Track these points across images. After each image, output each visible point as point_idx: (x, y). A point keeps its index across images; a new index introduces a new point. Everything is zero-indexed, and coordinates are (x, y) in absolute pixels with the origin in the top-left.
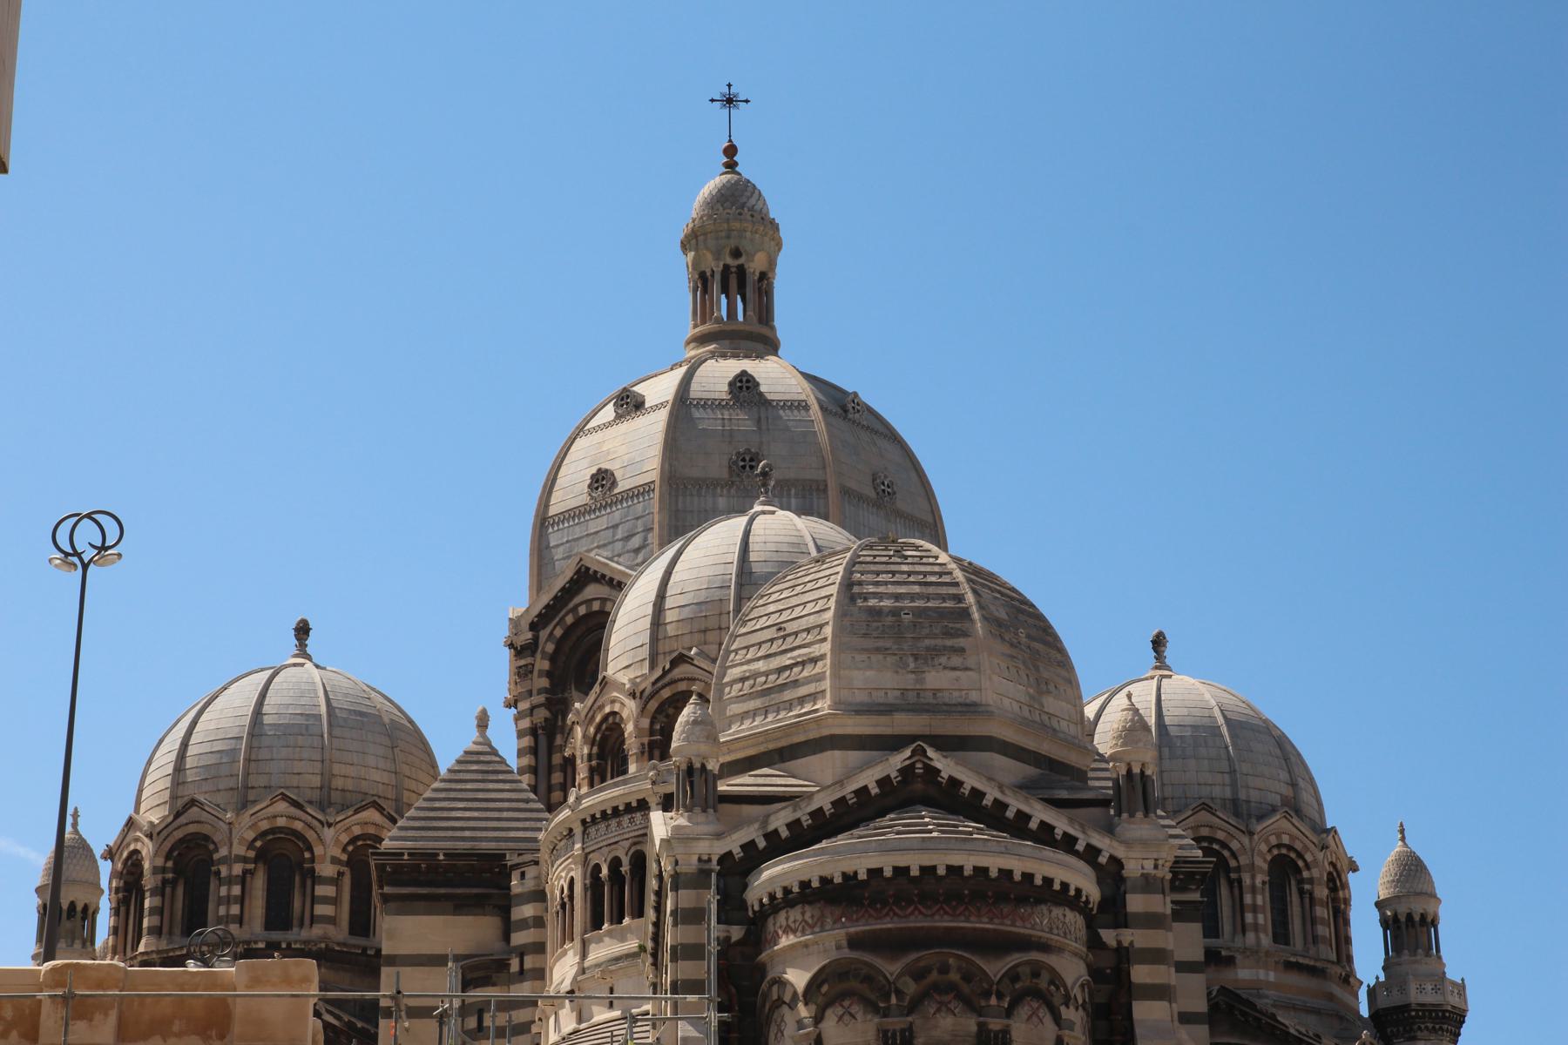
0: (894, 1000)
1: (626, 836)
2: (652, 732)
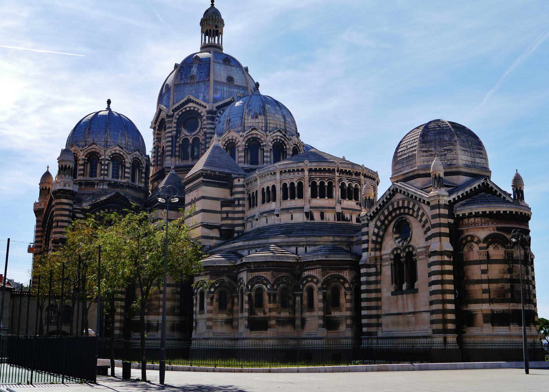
0: (509, 245)
2: (245, 146)
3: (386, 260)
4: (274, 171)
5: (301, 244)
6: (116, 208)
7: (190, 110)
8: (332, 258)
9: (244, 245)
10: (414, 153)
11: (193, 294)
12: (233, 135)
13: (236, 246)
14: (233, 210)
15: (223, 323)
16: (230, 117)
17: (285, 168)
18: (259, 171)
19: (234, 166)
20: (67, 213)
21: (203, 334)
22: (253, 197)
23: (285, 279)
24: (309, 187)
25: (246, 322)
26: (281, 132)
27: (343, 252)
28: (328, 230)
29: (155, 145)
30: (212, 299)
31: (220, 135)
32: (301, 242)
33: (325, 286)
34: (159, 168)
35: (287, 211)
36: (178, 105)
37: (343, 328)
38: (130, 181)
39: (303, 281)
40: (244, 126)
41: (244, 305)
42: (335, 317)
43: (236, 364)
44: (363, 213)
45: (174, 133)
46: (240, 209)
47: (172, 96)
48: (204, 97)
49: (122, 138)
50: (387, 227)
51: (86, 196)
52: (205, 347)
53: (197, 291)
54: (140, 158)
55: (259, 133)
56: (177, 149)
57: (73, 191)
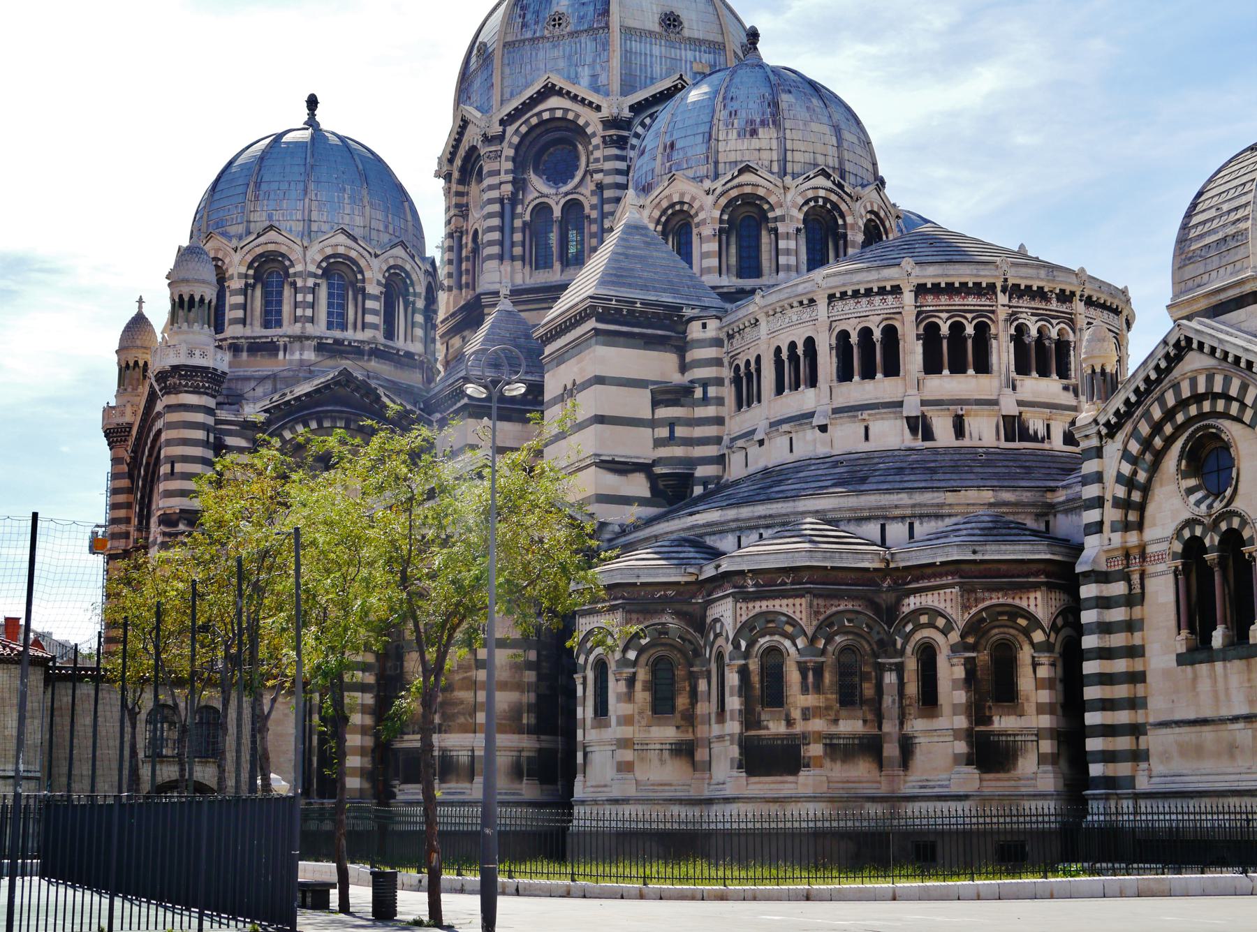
1: (879, 312)
2: (721, 221)
3: (1160, 558)
4: (810, 296)
5: (897, 512)
6: (341, 419)
7: (552, 119)
8: (993, 552)
9: (723, 519)
10: (1242, 226)
11: (573, 668)
12: (683, 189)
13: (701, 522)
14: (690, 416)
15: (666, 754)
16: (672, 135)
17: (844, 285)
18: (763, 297)
19: (689, 283)
20: (200, 435)
21: (605, 786)
22: (749, 375)
23: (849, 621)
24: (918, 339)
25: (735, 751)
26: (828, 176)
27: (1025, 535)
28: (979, 470)
29: (453, 227)
30: (631, 681)
31: (646, 189)
32: (896, 507)
33: (971, 640)
34: (467, 295)
35: (850, 414)
36: (515, 103)
37: (1027, 764)
38: (380, 336)
39: (904, 627)
40: (716, 163)
41: (728, 699)
42: (1004, 733)
43: (706, 874)
44: (1085, 416)
45: (508, 189)
46: (711, 411)
47: (496, 79)
48: (594, 77)
49: (353, 210)
50: (1159, 456)
51: (253, 384)
52: (613, 824)
53: (586, 660)
54: (408, 267)
55: (762, 183)
56: (518, 237)
57: (216, 370)
